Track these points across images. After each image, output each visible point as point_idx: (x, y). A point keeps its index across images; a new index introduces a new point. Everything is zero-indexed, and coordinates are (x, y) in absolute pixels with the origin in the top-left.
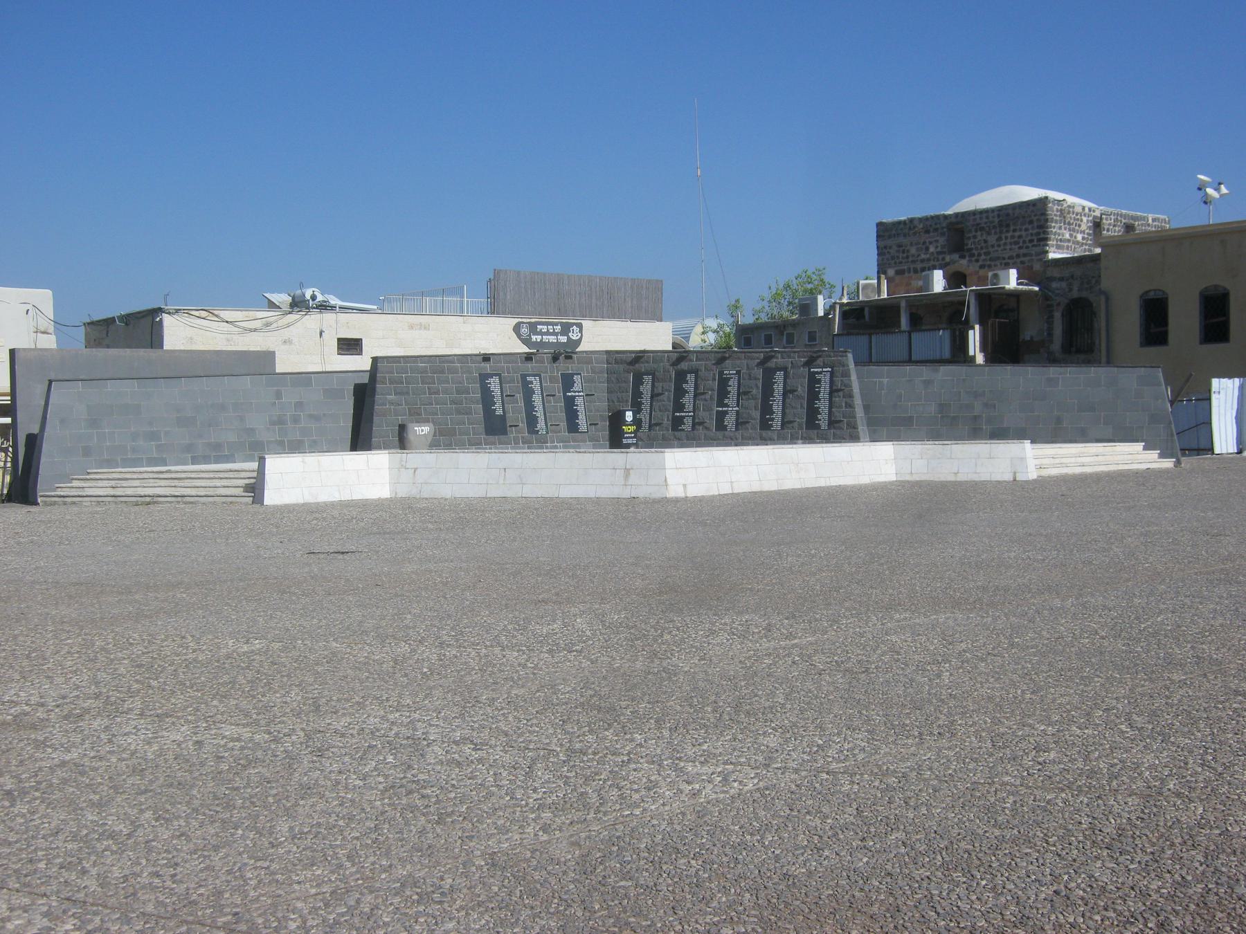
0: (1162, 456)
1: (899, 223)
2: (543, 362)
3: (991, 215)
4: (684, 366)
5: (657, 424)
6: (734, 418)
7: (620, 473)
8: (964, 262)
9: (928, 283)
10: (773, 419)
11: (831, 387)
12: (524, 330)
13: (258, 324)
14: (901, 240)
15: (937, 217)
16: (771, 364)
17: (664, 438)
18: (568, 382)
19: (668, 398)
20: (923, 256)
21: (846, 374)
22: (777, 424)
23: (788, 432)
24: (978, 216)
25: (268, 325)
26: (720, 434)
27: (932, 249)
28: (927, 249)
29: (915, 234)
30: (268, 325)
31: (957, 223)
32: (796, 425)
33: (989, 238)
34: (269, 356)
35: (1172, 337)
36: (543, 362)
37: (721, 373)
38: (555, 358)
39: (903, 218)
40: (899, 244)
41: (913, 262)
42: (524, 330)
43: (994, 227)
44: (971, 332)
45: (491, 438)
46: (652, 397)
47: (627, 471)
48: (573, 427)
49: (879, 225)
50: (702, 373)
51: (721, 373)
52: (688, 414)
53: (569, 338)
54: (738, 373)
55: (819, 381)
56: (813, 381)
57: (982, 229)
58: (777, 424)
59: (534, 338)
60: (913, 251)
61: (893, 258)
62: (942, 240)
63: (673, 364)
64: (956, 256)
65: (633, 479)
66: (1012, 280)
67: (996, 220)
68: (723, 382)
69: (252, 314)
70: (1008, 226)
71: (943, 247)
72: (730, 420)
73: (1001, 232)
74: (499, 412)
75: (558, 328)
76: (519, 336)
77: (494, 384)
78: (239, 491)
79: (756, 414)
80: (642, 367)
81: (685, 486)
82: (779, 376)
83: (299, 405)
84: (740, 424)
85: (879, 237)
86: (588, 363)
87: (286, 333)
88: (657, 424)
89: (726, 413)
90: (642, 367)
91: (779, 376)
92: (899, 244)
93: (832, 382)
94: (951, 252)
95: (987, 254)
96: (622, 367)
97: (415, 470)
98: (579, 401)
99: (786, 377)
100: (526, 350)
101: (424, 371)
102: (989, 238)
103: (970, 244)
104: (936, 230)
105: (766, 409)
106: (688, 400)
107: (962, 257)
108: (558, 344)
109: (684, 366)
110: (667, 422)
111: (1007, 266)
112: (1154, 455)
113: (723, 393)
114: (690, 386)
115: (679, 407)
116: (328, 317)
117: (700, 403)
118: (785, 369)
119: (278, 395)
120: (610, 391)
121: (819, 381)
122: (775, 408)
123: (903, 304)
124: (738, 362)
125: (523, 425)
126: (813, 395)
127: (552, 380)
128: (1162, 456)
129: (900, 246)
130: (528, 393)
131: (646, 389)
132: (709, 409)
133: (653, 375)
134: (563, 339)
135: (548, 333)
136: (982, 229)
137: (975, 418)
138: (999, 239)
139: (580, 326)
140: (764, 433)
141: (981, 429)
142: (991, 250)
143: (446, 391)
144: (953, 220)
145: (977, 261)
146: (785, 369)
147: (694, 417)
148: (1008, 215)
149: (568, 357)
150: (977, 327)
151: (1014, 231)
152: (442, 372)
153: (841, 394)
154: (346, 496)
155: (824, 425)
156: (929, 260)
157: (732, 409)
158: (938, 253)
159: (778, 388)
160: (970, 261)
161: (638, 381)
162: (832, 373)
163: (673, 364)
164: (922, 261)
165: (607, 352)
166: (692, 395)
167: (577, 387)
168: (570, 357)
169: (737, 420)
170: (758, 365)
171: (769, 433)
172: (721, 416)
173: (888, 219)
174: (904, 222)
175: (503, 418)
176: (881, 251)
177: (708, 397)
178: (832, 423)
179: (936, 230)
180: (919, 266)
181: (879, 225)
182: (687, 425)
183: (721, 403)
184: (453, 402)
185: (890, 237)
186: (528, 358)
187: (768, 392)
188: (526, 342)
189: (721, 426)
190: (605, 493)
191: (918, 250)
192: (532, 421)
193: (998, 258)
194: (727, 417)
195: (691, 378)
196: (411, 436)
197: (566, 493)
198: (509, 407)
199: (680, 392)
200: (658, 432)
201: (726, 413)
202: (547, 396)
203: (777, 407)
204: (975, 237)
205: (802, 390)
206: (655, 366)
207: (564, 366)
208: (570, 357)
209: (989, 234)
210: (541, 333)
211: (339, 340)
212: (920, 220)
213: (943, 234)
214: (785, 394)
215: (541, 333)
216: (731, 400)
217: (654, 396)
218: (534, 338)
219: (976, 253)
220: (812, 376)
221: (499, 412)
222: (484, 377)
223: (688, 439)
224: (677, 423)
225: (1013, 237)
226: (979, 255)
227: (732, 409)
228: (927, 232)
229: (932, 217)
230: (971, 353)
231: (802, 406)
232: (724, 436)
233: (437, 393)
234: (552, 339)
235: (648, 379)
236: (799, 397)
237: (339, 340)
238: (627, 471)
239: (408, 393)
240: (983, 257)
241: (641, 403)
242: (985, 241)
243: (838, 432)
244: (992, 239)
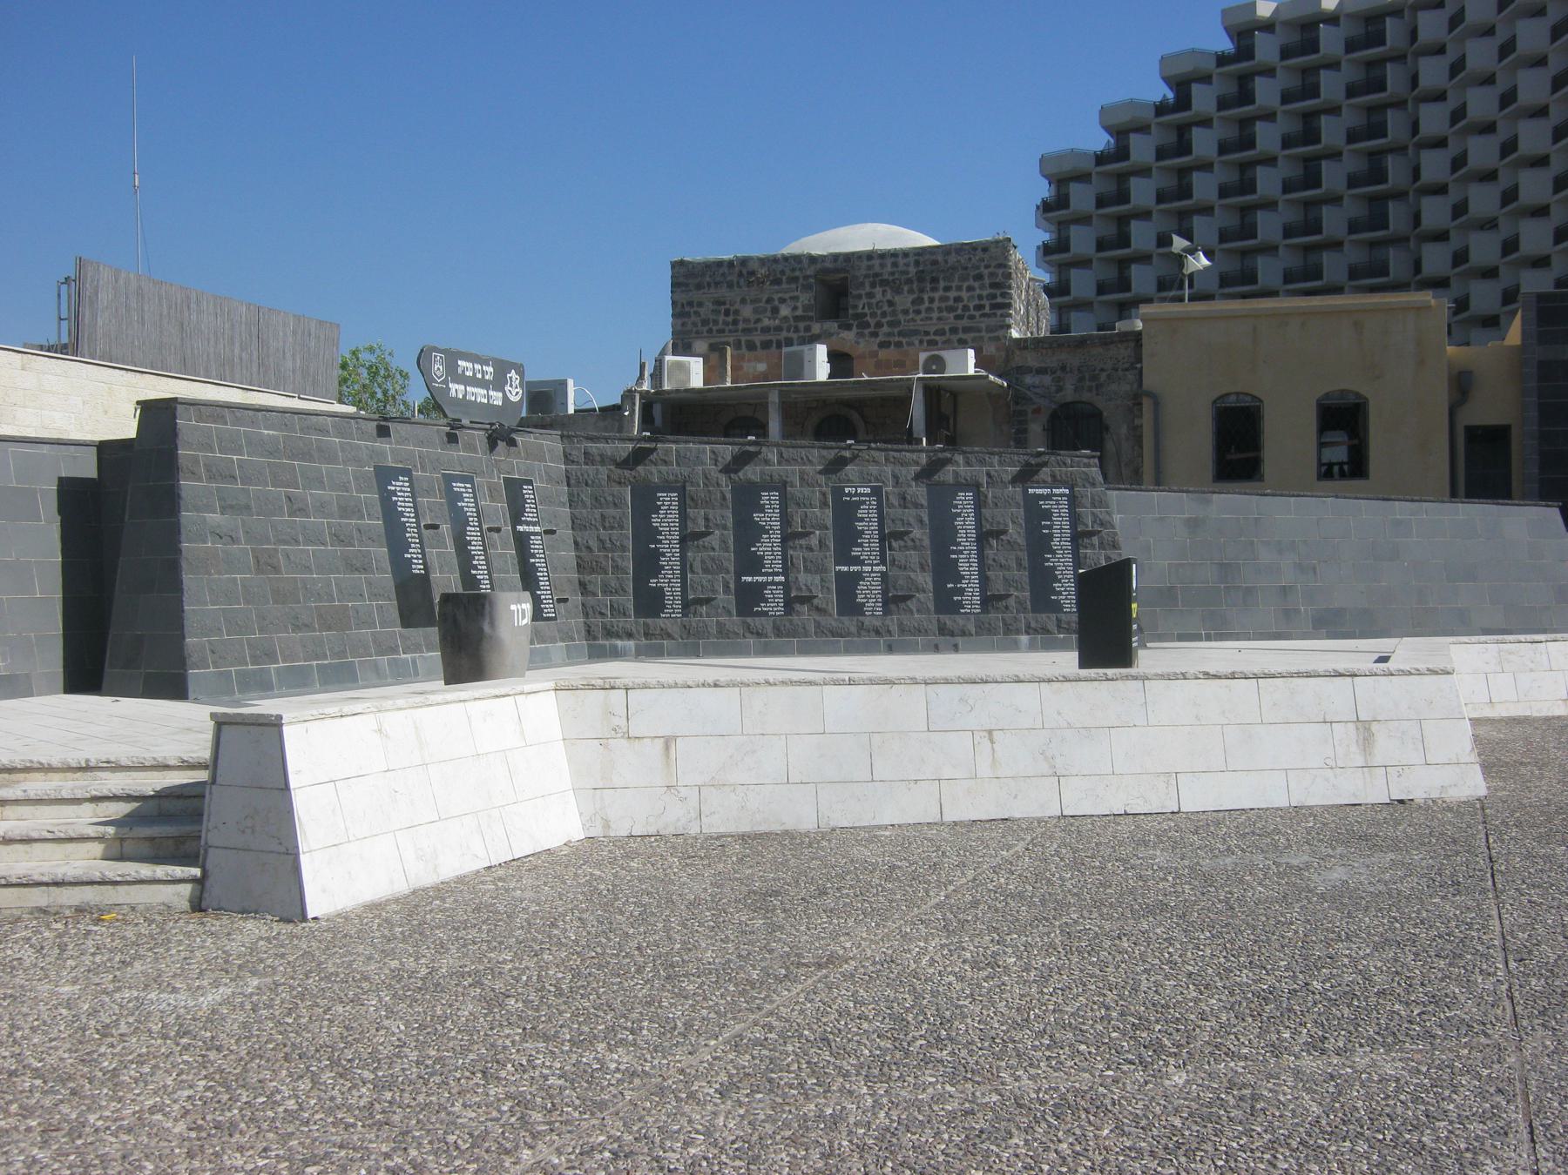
1: (720, 264)
3: (901, 261)
5: (699, 602)
6: (877, 588)
7: (1345, 734)
8: (849, 336)
9: (800, 365)
10: (961, 592)
11: (1073, 526)
14: (723, 292)
16: (947, 475)
17: (722, 632)
19: (720, 543)
20: (766, 322)
21: (1099, 502)
22: (971, 598)
23: (994, 616)
24: (876, 262)
26: (849, 623)
27: (785, 311)
28: (775, 310)
29: (749, 284)
31: (837, 271)
32: (1012, 602)
33: (897, 299)
37: (838, 492)
39: (726, 257)
40: (709, 298)
41: (747, 331)
43: (909, 281)
46: (683, 540)
47: (1365, 730)
49: (678, 266)
50: (796, 490)
52: (771, 576)
53: (505, 397)
54: (876, 492)
55: (1047, 515)
56: (1036, 515)
57: (884, 283)
58: (971, 598)
60: (747, 311)
61: (705, 322)
62: (805, 298)
63: (727, 470)
65: (1386, 748)
66: (968, 364)
67: (912, 270)
68: (845, 513)
70: (934, 280)
71: (806, 308)
72: (869, 593)
73: (922, 291)
74: (418, 569)
78: (84, 861)
79: (926, 580)
82: (964, 500)
84: (893, 600)
85: (675, 285)
88: (699, 602)
89: (859, 576)
91: (964, 500)
92: (709, 298)
93: (1075, 519)
95: (891, 324)
96: (604, 471)
97: (668, 742)
98: (536, 543)
99: (979, 504)
102: (897, 299)
103: (861, 306)
104: (795, 280)
105: (945, 570)
106: (768, 548)
107: (848, 327)
108: (489, 406)
110: (726, 599)
111: (963, 344)
113: (847, 537)
114: (769, 516)
115: (753, 564)
117: (798, 555)
118: (974, 486)
120: (576, 524)
121: (1047, 515)
122: (963, 567)
123: (774, 398)
124: (873, 469)
126: (1039, 544)
129: (719, 303)
131: (666, 519)
133: (682, 492)
136: (884, 283)
137: (1284, 591)
138: (918, 301)
140: (946, 618)
141: (1297, 611)
142: (901, 317)
143: (322, 508)
144: (828, 265)
145: (875, 335)
146: (974, 486)
147: (786, 586)
148: (935, 263)
151: (947, 289)
153: (1095, 540)
156: (778, 329)
157: (872, 572)
158: (797, 318)
159: (966, 526)
160: (860, 335)
161: (645, 502)
162: (1073, 500)
163: (727, 470)
164: (766, 330)
166: (776, 538)
169: (885, 592)
170: (917, 477)
171: (960, 621)
172: (847, 585)
173: (698, 254)
174: (731, 264)
176: (681, 311)
177: (814, 541)
179: (795, 279)
180: (758, 339)
181: (678, 266)
182: (774, 603)
183: (844, 557)
184: (338, 539)
185: (699, 287)
187: (943, 536)
189: (848, 604)
190: (1319, 791)
191: (755, 311)
193: (915, 332)
194: (862, 586)
195: (770, 499)
197: (1199, 797)
198: (432, 552)
199: (747, 532)
201: (859, 576)
203: (968, 565)
204: (870, 295)
206: (685, 471)
209: (898, 291)
212: (763, 261)
213: (807, 288)
214: (983, 538)
216: (867, 548)
217: (687, 539)
219: (872, 322)
220: (1031, 504)
223: (778, 632)
224: (749, 599)
225: (943, 299)
226: (879, 325)
227: (872, 572)
228: (777, 282)
231: (1019, 565)
232: (861, 627)
233: (302, 511)
235: (668, 501)
238: (1365, 730)
240: (886, 329)
241: (657, 554)
242: (891, 303)
244: (904, 301)
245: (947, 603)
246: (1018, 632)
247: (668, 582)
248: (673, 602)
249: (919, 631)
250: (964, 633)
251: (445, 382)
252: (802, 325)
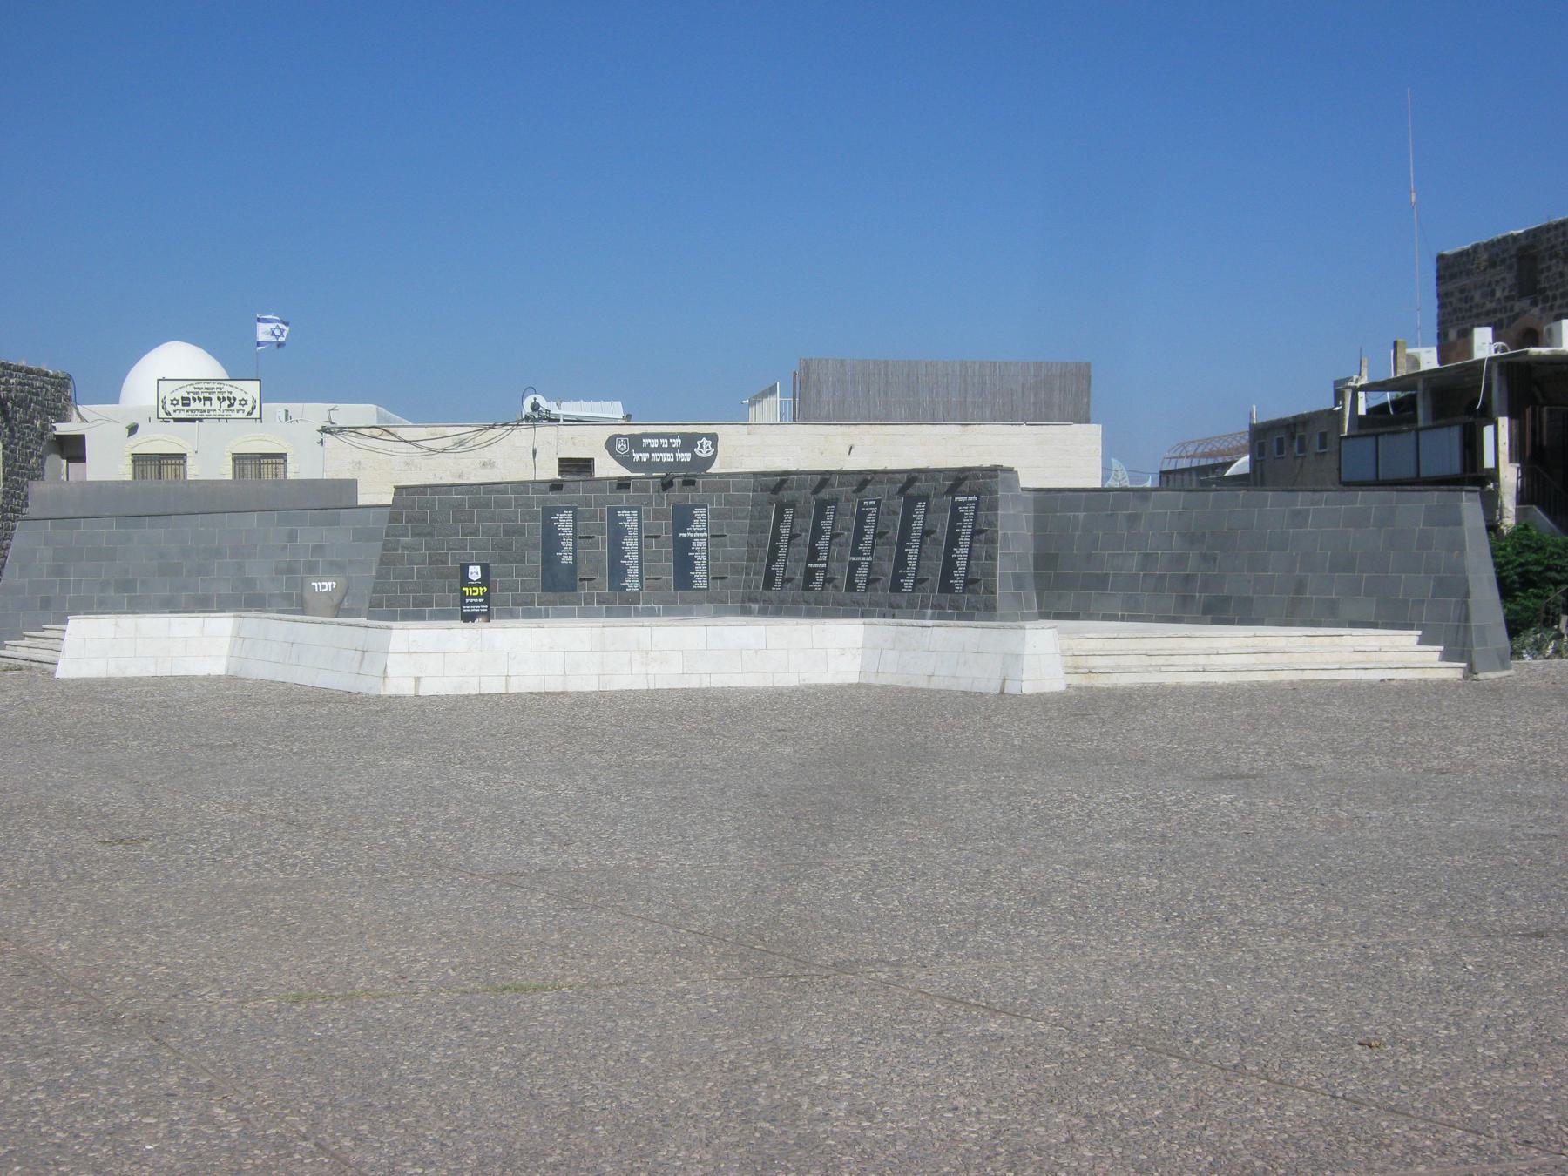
0: (1446, 657)
2: (647, 491)
4: (825, 494)
8: (1536, 311)
12: (622, 447)
13: (447, 443)
15: (1505, 239)
18: (683, 518)
22: (908, 583)
24: (1552, 233)
25: (461, 443)
27: (1498, 294)
30: (461, 443)
34: (350, 486)
35: (129, 461)
36: (647, 491)
37: (861, 504)
38: (667, 484)
39: (1465, 247)
42: (622, 447)
44: (1488, 431)
45: (550, 596)
48: (683, 578)
51: (861, 504)
53: (694, 456)
54: (878, 502)
56: (956, 516)
59: (637, 457)
62: (1510, 278)
64: (1526, 302)
69: (441, 431)
72: (861, 576)
74: (567, 559)
75: (677, 442)
76: (613, 453)
77: (564, 522)
80: (785, 495)
81: (417, 679)
83: (318, 548)
86: (723, 490)
87: (486, 454)
90: (785, 495)
94: (1522, 296)
100: (624, 472)
101: (461, 505)
106: (822, 545)
107: (1534, 303)
108: (677, 465)
109: (825, 494)
110: (799, 577)
112: (1433, 654)
113: (859, 535)
115: (813, 555)
116: (546, 431)
119: (292, 536)
125: (602, 579)
127: (658, 515)
128: (1446, 657)
129: (1462, 291)
130: (618, 534)
132: (841, 559)
134: (685, 457)
135: (660, 449)
137: (1188, 579)
139: (713, 438)
141: (1193, 597)
144: (1524, 243)
149: (689, 483)
150: (1504, 422)
152: (487, 506)
154: (164, 671)
155: (958, 584)
159: (917, 527)
160: (1543, 310)
165: (755, 474)
166: (827, 537)
167: (698, 524)
168: (693, 483)
175: (572, 569)
178: (969, 583)
179: (1503, 261)
186: (623, 484)
188: (626, 462)
189: (851, 586)
192: (617, 571)
196: (307, 596)
198: (583, 554)
199: (817, 532)
200: (790, 592)
202: (648, 537)
205: (941, 532)
207: (677, 494)
208: (693, 483)
210: (649, 450)
211: (561, 461)
213: (1510, 267)
215: (649, 450)
217: (793, 537)
218: (637, 457)
219: (1550, 294)
221: (567, 559)
222: (549, 512)
226: (1555, 298)
229: (1499, 241)
230: (1489, 462)
233: (475, 533)
234: (667, 457)
236: (937, 542)
237: (561, 461)
239: (431, 534)
240: (1559, 302)
243: (973, 598)
245: (896, 586)
246: (926, 606)
247: (778, 567)
248: (778, 580)
249: (878, 604)
250: (899, 607)
251: (630, 453)
252: (1509, 305)
